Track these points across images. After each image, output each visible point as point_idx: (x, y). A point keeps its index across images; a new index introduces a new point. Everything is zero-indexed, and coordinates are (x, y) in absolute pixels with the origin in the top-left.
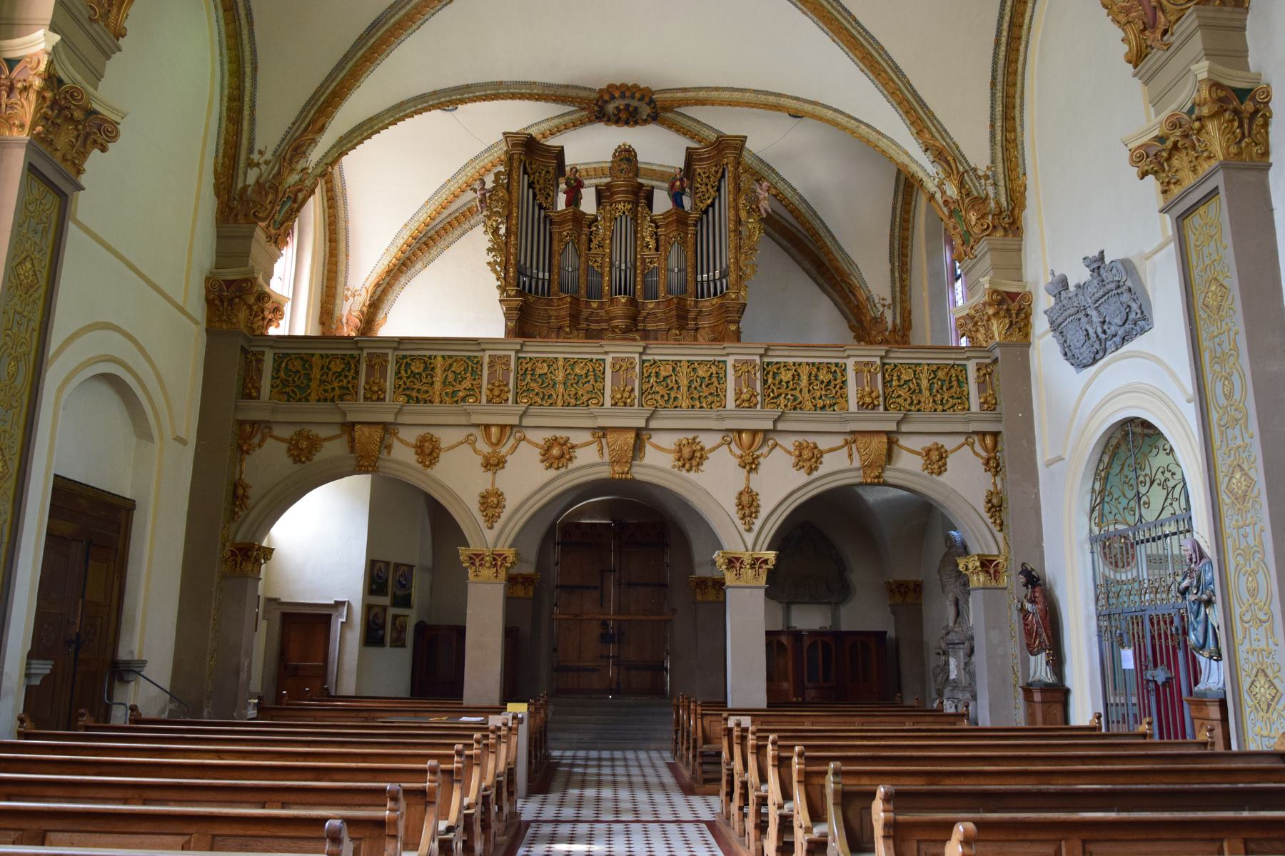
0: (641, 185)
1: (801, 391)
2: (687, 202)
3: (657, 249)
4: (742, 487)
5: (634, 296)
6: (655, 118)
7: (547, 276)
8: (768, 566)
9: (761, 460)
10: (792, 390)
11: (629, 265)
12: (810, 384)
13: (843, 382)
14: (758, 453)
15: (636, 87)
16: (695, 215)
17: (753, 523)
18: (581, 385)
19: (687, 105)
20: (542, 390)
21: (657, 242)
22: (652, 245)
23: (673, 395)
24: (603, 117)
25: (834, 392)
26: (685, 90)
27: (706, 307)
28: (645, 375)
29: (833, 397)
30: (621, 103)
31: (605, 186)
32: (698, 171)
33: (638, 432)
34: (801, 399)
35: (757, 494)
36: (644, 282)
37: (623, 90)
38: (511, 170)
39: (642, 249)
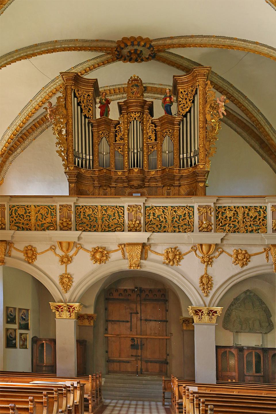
0: (146, 101)
1: (238, 222)
2: (174, 109)
3: (156, 140)
4: (203, 273)
5: (143, 168)
6: (153, 56)
7: (91, 157)
8: (217, 315)
9: (214, 259)
10: (233, 221)
11: (139, 150)
12: (244, 218)
13: (264, 217)
14: (212, 256)
15: (140, 38)
16: (178, 118)
17: (209, 292)
18: (111, 220)
19: (173, 47)
20: (90, 223)
21: (156, 136)
22: (153, 137)
23: (163, 225)
24: (121, 58)
25: (258, 223)
26: (172, 38)
27: (186, 173)
28: (147, 214)
29: (258, 225)
30: (130, 48)
31: (123, 102)
32: (181, 90)
33: (144, 245)
34: (238, 226)
35: (211, 277)
36: (148, 159)
37: (132, 40)
38: (66, 95)
39: (147, 140)
